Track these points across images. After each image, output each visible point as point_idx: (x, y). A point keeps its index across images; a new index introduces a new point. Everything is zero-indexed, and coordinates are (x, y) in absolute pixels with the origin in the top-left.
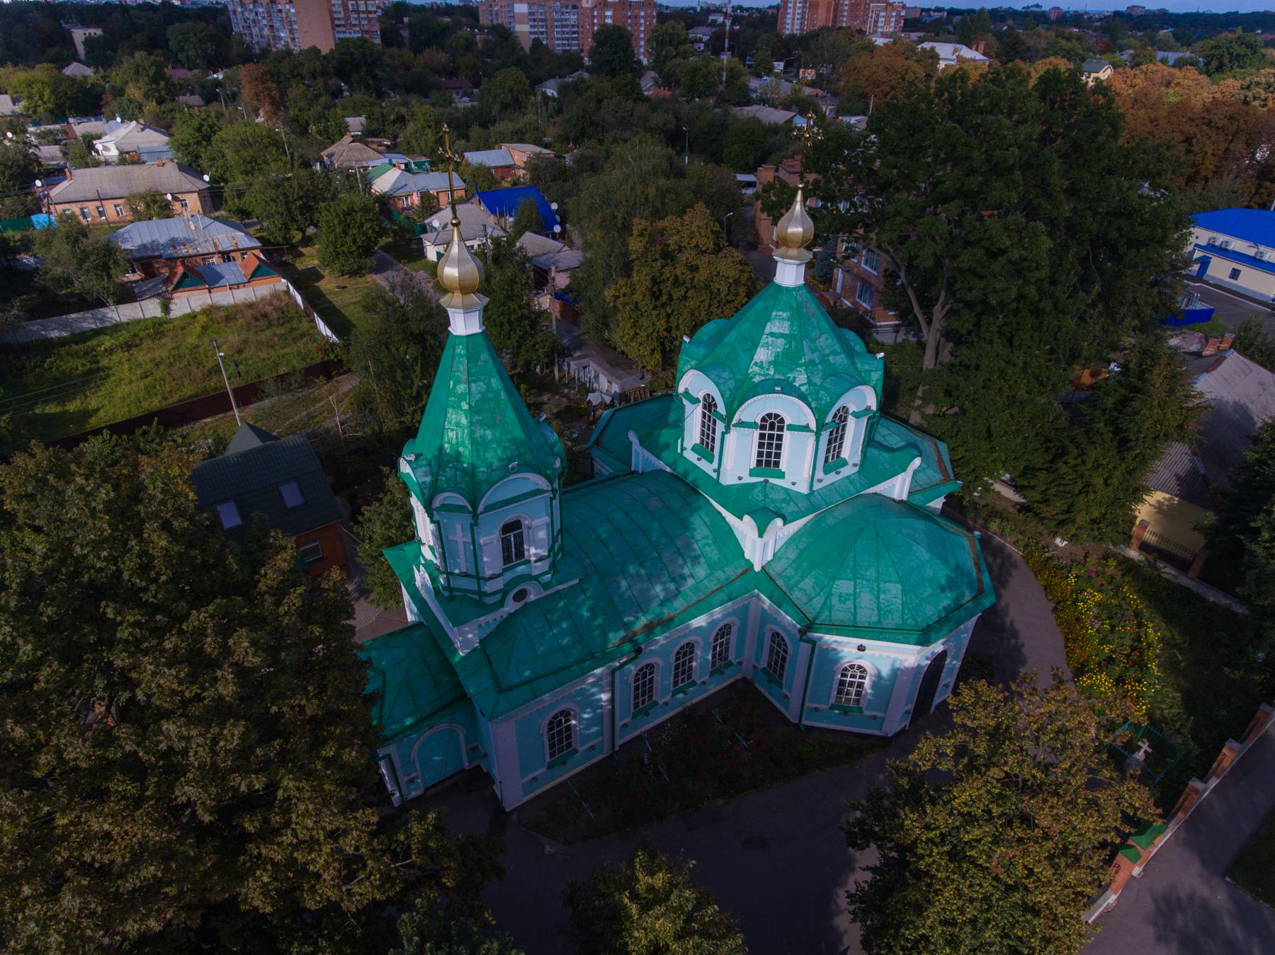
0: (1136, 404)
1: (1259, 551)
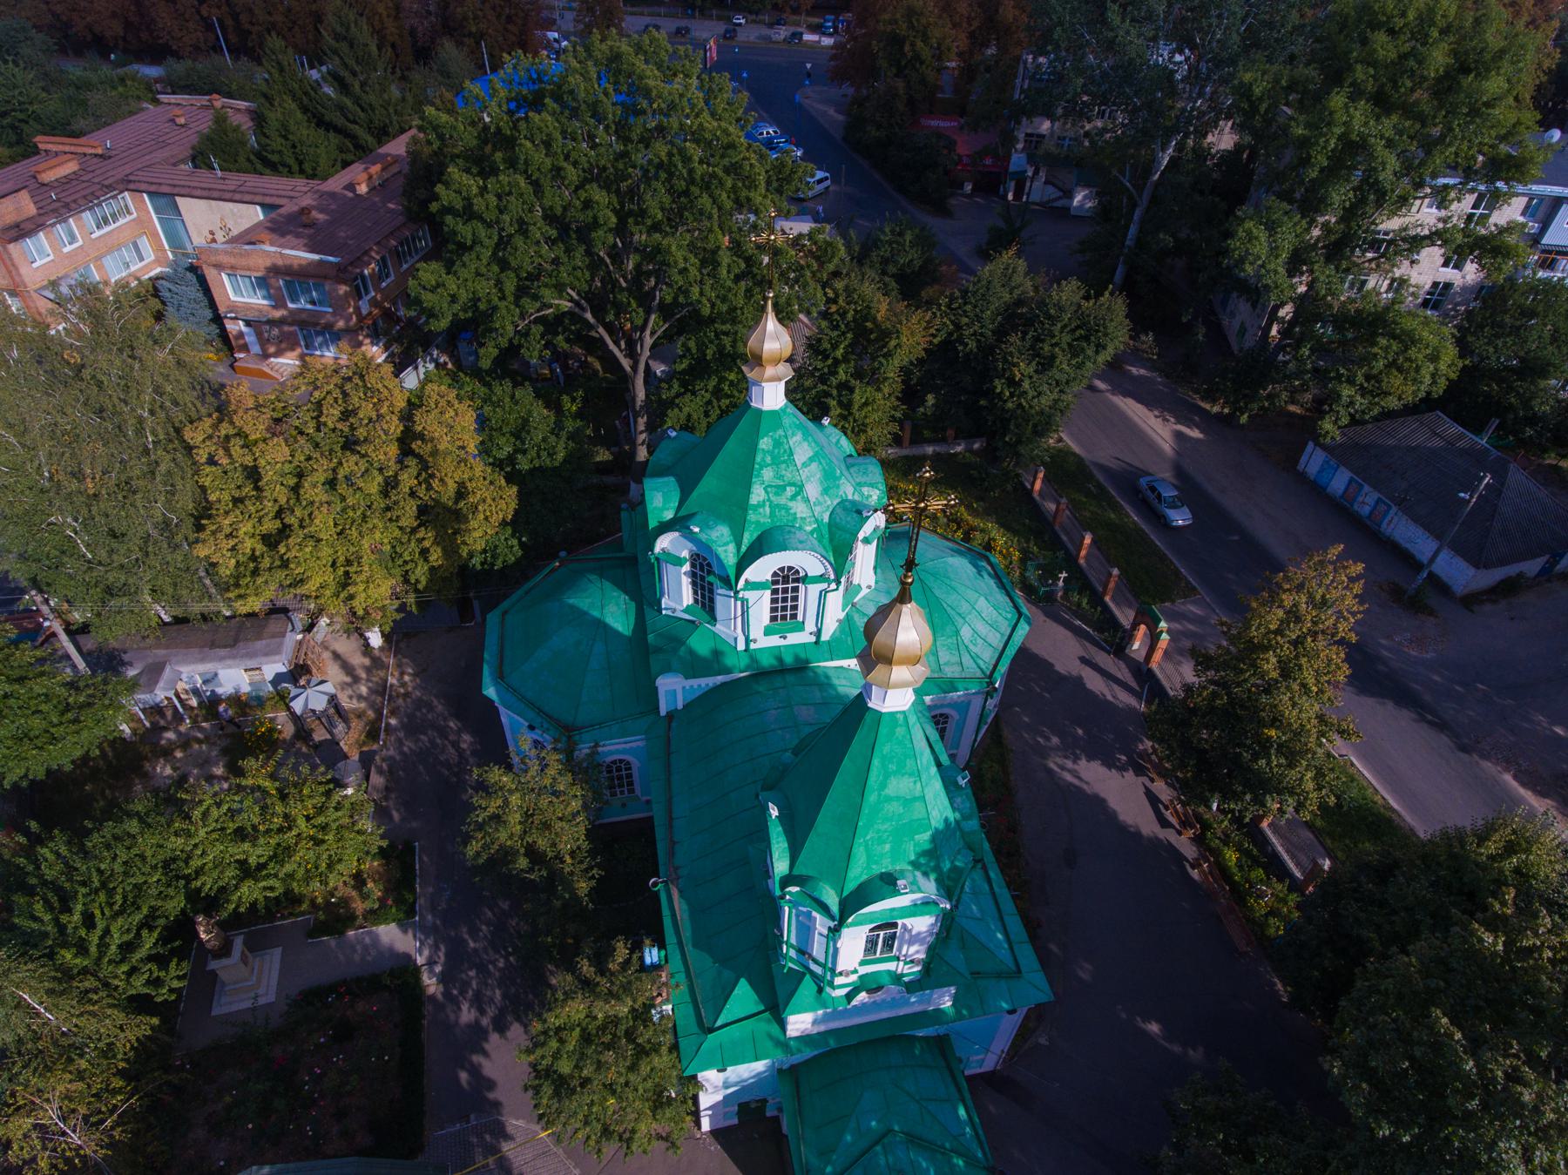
0: (893, 343)
1: (1010, 405)
